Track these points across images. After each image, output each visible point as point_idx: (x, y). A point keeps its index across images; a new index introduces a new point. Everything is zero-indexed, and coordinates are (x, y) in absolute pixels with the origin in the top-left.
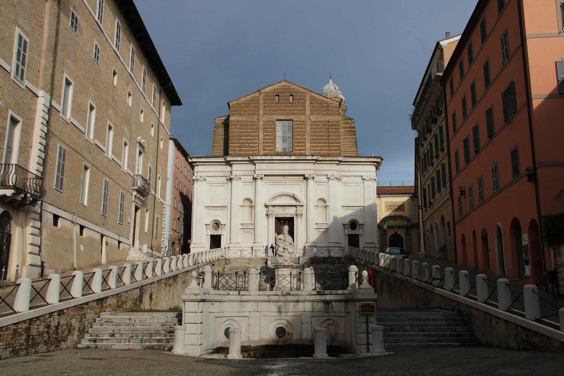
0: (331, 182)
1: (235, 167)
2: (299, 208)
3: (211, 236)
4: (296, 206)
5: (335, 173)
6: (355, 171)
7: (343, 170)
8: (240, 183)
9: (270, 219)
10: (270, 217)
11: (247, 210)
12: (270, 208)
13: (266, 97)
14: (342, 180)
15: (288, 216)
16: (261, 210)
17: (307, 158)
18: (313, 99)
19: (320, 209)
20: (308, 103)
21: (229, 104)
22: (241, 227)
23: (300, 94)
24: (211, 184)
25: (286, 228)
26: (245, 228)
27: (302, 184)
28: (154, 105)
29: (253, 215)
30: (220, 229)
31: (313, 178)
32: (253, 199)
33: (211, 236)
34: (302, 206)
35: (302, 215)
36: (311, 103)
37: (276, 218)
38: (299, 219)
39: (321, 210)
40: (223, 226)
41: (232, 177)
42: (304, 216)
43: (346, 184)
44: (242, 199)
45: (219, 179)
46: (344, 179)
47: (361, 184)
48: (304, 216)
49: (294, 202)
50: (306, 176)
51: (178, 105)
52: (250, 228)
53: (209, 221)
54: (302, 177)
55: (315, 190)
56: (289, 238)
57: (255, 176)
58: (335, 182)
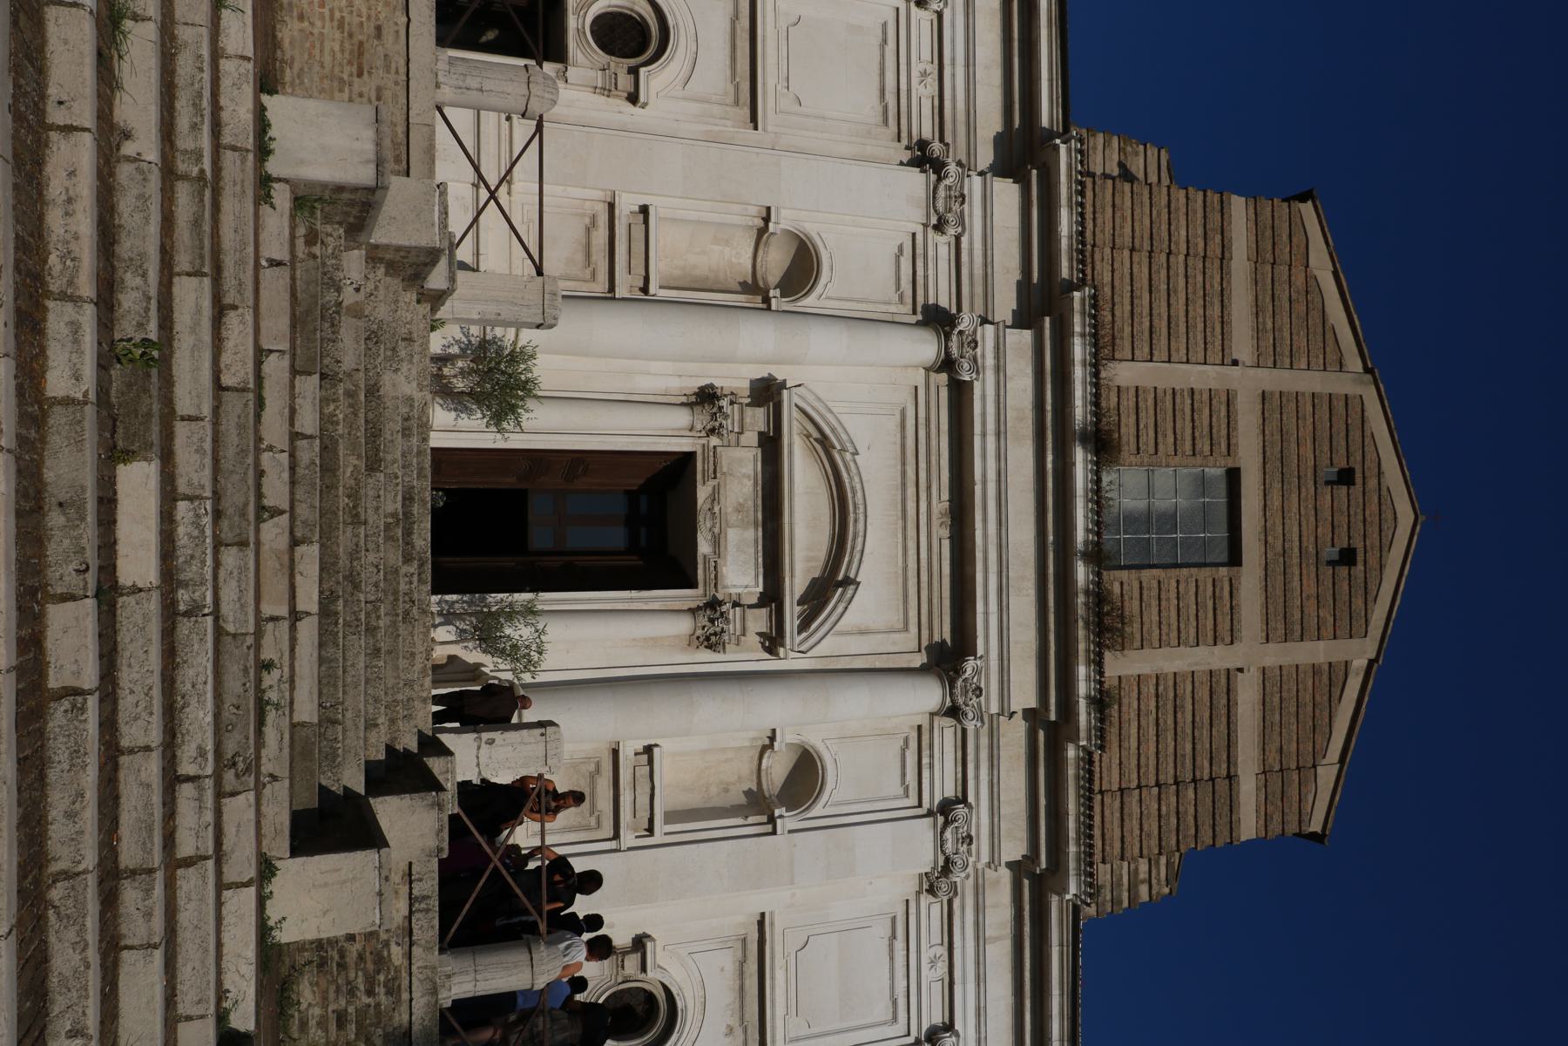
0: (923, 831)
1: (1006, 193)
2: (759, 621)
4: (772, 596)
6: (980, 980)
7: (990, 899)
8: (912, 217)
9: (682, 418)
10: (702, 419)
11: (736, 257)
12: (757, 419)
13: (1340, 406)
14: (926, 899)
15: (704, 547)
16: (742, 349)
17: (1082, 671)
18: (1335, 675)
19: (745, 766)
20: (1316, 652)
21: (1303, 198)
22: (627, 205)
23: (1358, 602)
26: (621, 235)
27: (909, 640)
29: (698, 295)
30: (602, 57)
31: (954, 712)
32: (810, 302)
34: (773, 642)
35: (712, 642)
36: (1315, 670)
37: (689, 457)
38: (684, 625)
39: (737, 775)
40: (625, 82)
41: (952, 168)
42: (706, 661)
43: (902, 929)
44: (811, 228)
45: (924, 92)
46: (933, 910)
47: (900, 1028)
48: (706, 661)
49: (797, 582)
50: (970, 665)
52: (621, 265)
54: (944, 632)
55: (867, 728)
57: (966, 323)
58: (924, 857)
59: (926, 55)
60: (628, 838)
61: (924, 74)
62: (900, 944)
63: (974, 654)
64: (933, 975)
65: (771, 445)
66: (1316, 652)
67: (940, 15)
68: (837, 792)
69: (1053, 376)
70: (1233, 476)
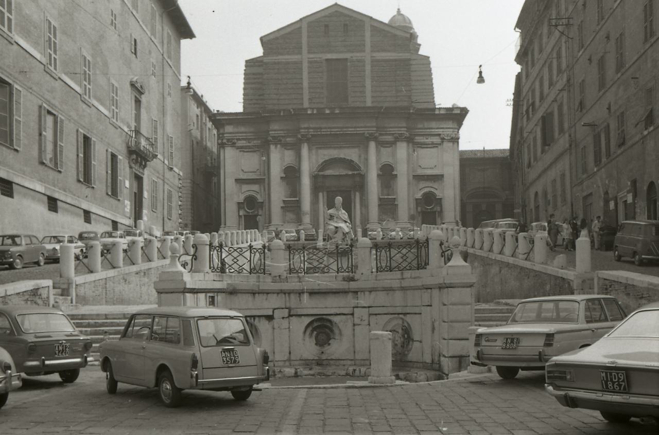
2: (357, 179)
3: (244, 216)
5: (403, 131)
20: (368, 34)
24: (241, 149)
25: (339, 199)
28: (154, 34)
33: (244, 216)
41: (270, 138)
51: (191, 39)
53: (241, 198)
56: (344, 214)
57: (299, 136)
59: (245, 142)
60: (396, 203)
61: (249, 142)
62: (423, 146)
63: (364, 133)
64: (430, 140)
65: (325, 177)
66: (368, 34)
67: (237, 139)
68: (390, 160)
69: (311, 117)
70: (327, 60)
